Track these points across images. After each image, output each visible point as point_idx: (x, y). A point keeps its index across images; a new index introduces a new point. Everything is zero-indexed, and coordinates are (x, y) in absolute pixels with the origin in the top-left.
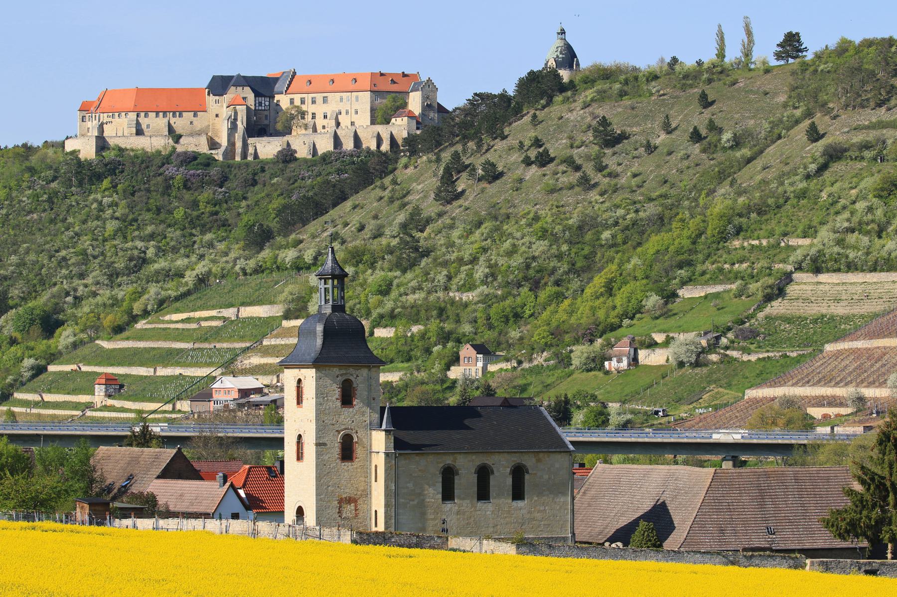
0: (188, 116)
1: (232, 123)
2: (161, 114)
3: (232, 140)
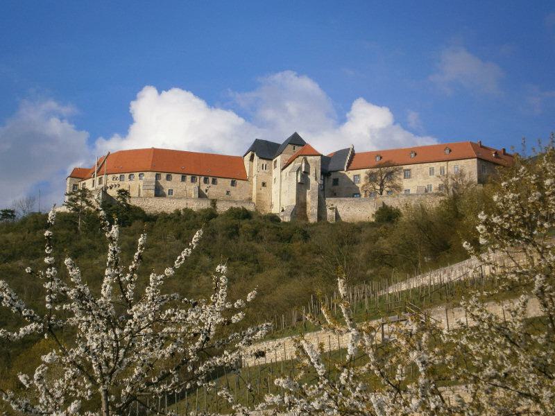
0: (224, 183)
1: (302, 176)
2: (189, 178)
3: (301, 199)
